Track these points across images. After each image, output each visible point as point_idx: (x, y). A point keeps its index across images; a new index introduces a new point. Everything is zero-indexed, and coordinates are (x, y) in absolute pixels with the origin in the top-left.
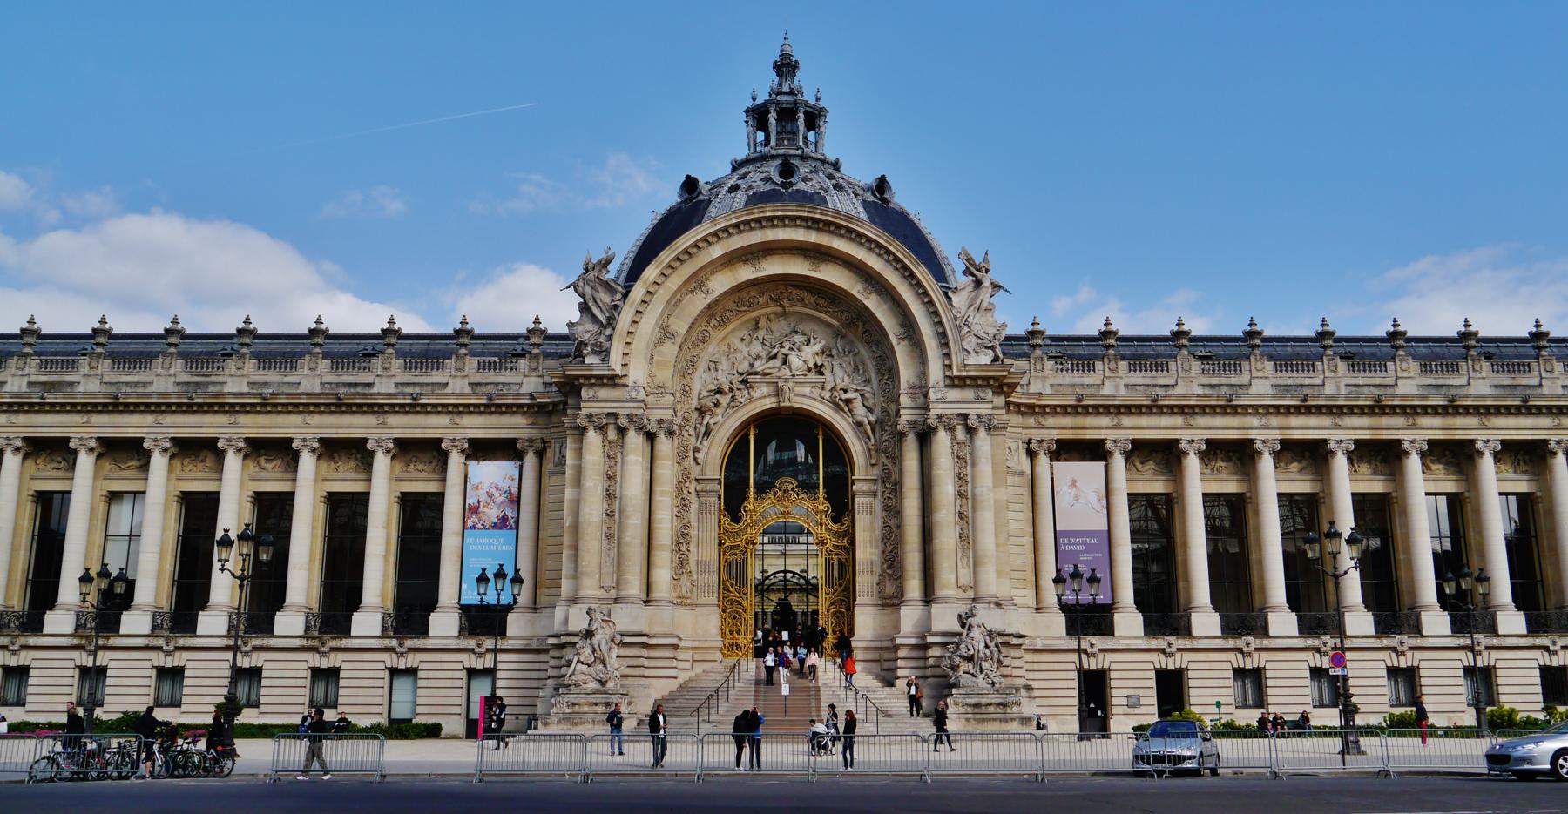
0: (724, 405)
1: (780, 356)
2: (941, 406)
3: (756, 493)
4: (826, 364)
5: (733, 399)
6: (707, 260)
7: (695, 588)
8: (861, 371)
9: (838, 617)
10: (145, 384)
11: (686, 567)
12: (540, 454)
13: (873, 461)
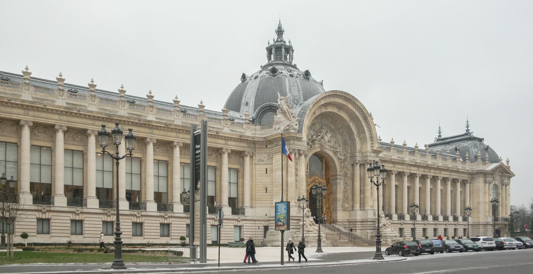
2: (370, 157)
5: (311, 147)
6: (320, 104)
10: (116, 112)
12: (251, 157)
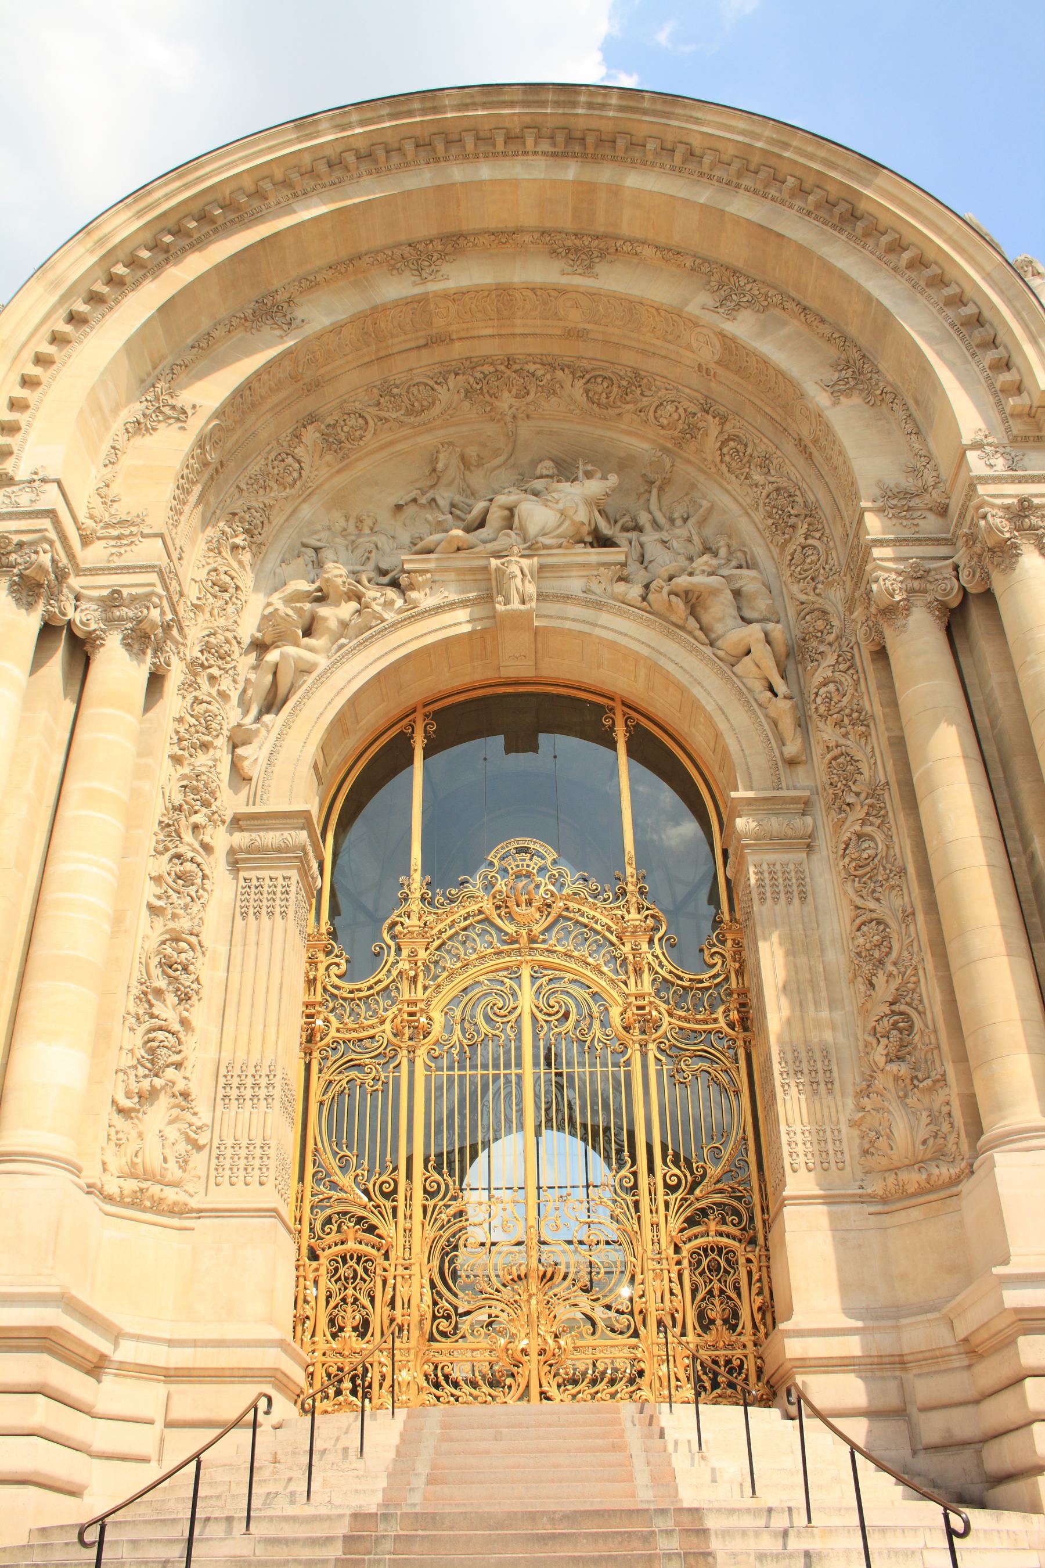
0: (333, 624)
1: (496, 516)
7: (199, 1160)
8: (723, 552)
9: (715, 1268)
11: (170, 1073)
13: (792, 748)
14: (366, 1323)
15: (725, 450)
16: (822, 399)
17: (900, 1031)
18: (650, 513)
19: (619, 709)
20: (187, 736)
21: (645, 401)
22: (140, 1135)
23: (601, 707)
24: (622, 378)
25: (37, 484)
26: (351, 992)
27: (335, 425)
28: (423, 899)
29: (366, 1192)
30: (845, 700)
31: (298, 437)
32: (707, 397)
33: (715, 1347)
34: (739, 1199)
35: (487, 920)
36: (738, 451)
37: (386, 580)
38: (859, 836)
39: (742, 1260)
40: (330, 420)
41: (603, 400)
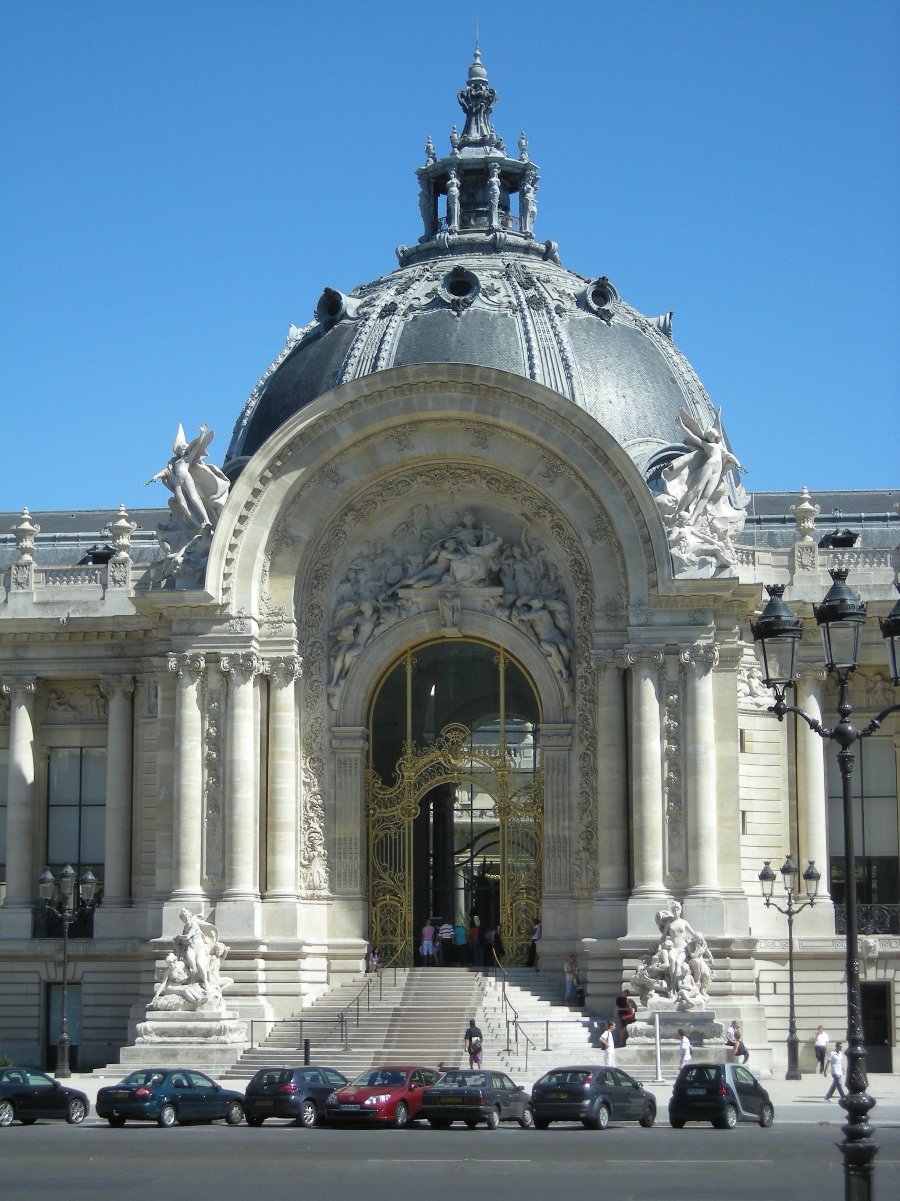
3: (416, 746)
4: (505, 568)
8: (553, 578)
14: (395, 929)
15: (554, 531)
16: (588, 543)
17: (588, 838)
18: (520, 545)
19: (502, 653)
20: (309, 700)
21: (517, 496)
22: (311, 874)
23: (494, 650)
24: (506, 481)
25: (242, 619)
26: (384, 795)
27: (361, 509)
28: (413, 752)
29: (393, 880)
30: (588, 687)
31: (343, 520)
32: (547, 498)
33: (523, 940)
34: (536, 885)
35: (440, 763)
36: (559, 533)
37: (390, 592)
38: (585, 754)
39: (536, 909)
40: (359, 507)
41: (496, 490)
